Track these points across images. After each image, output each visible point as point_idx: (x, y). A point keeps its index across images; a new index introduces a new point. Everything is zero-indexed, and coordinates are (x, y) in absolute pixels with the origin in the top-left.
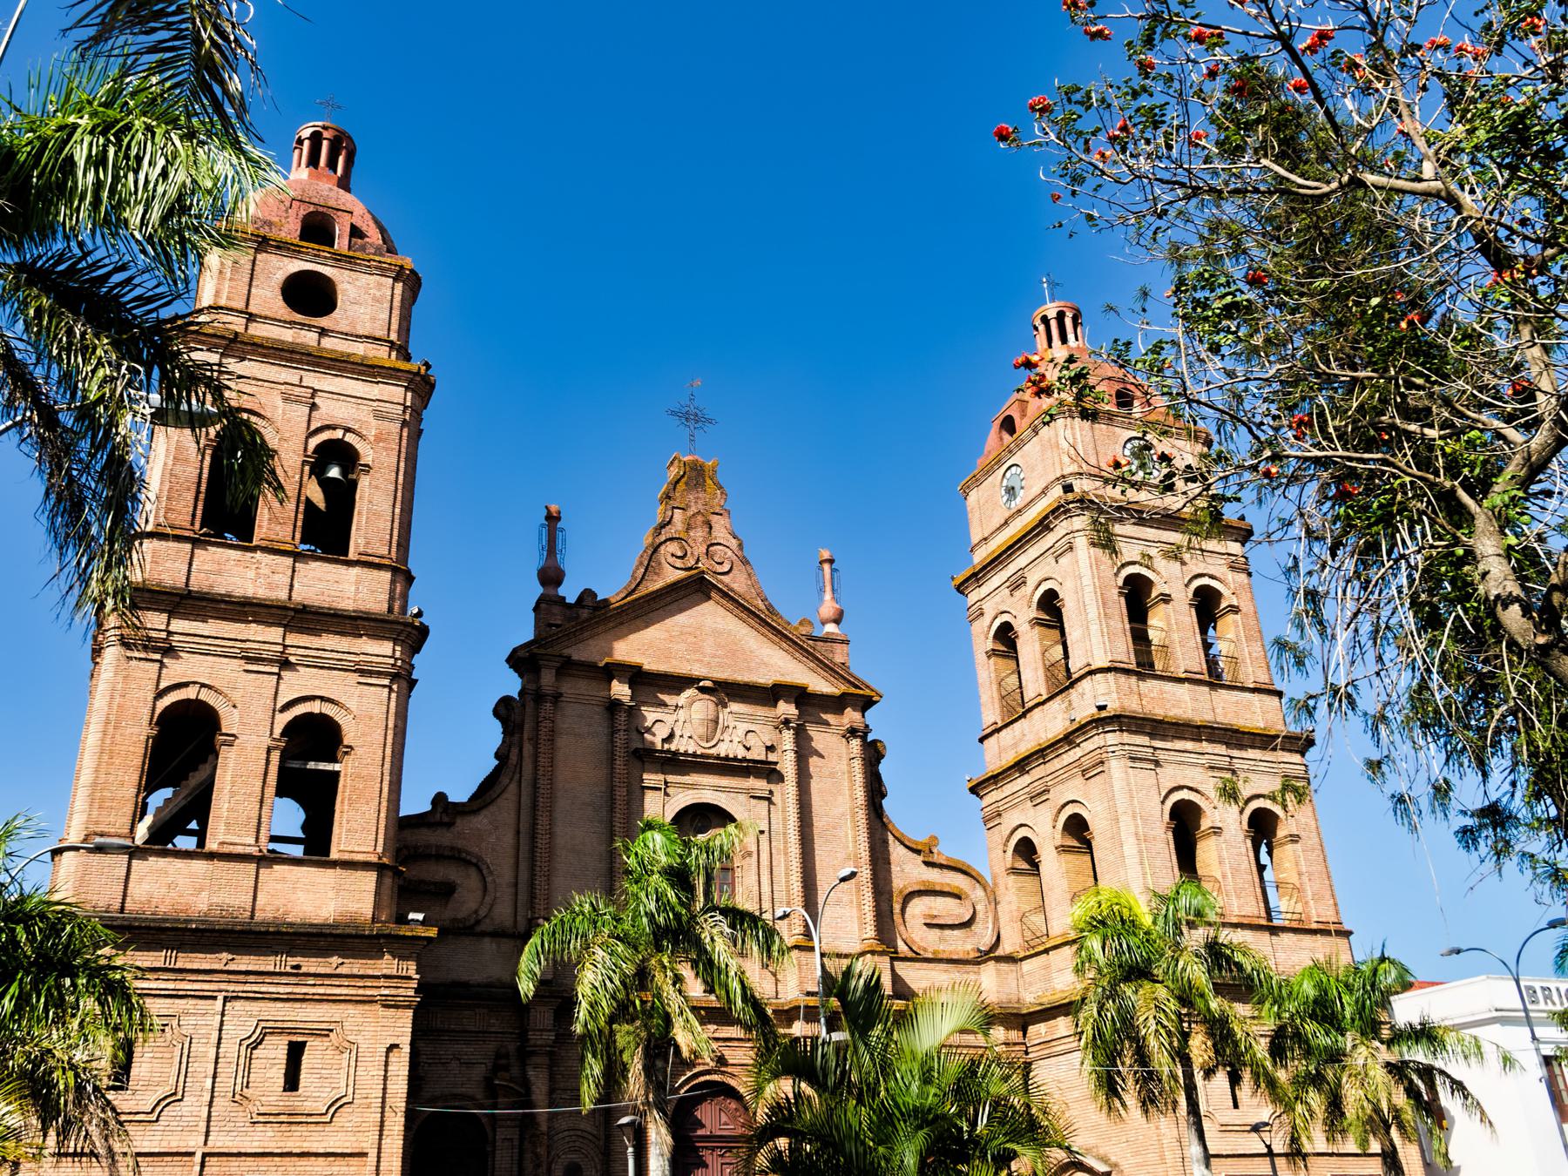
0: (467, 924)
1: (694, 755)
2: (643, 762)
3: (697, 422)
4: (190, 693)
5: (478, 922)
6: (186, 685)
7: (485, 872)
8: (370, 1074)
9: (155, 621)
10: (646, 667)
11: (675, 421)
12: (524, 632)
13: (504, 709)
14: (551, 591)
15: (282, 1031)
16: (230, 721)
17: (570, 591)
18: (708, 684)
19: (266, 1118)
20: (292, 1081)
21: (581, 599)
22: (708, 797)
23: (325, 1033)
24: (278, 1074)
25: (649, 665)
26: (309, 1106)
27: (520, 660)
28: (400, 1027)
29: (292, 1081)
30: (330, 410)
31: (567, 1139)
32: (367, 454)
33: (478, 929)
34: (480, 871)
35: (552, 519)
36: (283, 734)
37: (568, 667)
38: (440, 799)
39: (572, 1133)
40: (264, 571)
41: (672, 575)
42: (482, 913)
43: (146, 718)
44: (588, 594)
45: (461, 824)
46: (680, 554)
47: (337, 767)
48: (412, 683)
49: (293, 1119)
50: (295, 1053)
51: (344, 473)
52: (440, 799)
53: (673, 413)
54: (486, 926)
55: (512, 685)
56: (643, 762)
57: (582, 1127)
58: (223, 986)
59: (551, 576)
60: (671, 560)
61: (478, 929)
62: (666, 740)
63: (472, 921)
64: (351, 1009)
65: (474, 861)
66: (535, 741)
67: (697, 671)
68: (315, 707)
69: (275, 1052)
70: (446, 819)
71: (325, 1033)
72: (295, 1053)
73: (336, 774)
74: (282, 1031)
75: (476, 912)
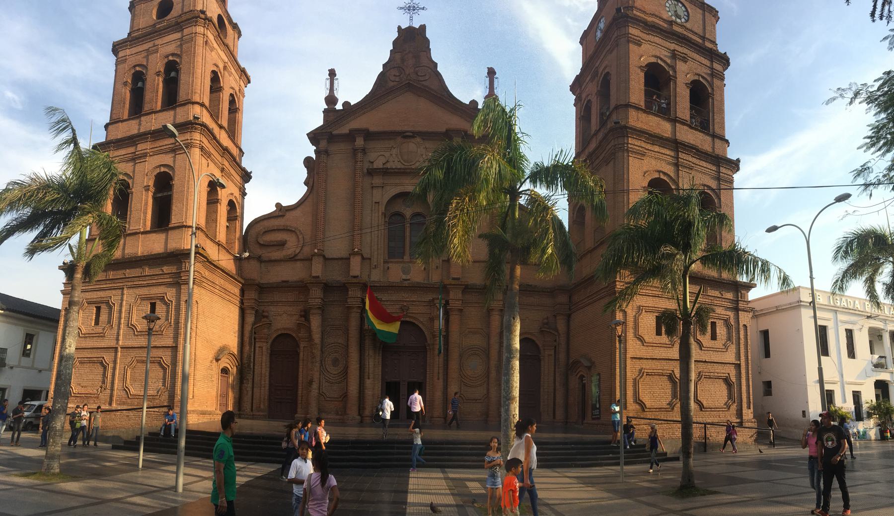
0: (291, 256)
1: (400, 169)
2: (372, 176)
3: (414, 10)
5: (296, 255)
7: (298, 233)
11: (402, 11)
18: (407, 134)
25: (373, 129)
27: (314, 137)
31: (334, 347)
33: (296, 258)
34: (296, 233)
39: (336, 344)
42: (297, 251)
45: (289, 215)
46: (398, 74)
52: (278, 205)
53: (401, 8)
54: (299, 257)
56: (372, 176)
57: (339, 341)
61: (296, 258)
63: (293, 255)
65: (293, 230)
66: (318, 173)
67: (406, 128)
70: (280, 214)
75: (295, 252)
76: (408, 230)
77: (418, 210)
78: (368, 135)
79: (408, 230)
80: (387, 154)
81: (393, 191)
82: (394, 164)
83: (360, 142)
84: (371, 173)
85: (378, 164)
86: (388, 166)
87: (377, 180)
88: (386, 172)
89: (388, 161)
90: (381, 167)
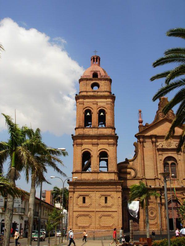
4: (86, 150)
6: (85, 149)
8: (116, 201)
9: (79, 141)
10: (157, 135)
12: (137, 131)
13: (135, 145)
14: (141, 124)
15: (104, 196)
16: (92, 153)
17: (144, 124)
19: (103, 207)
20: (106, 202)
21: (146, 125)
22: (170, 155)
23: (109, 196)
24: (104, 201)
26: (108, 205)
28: (120, 195)
29: (106, 202)
30: (99, 104)
32: (106, 110)
35: (140, 112)
36: (99, 155)
37: (144, 137)
38: (126, 159)
40: (94, 131)
41: (161, 119)
43: (80, 154)
44: (147, 124)
47: (107, 158)
48: (117, 145)
49: (107, 207)
50: (106, 198)
51: (103, 114)
52: (126, 159)
55: (136, 140)
58: (95, 190)
59: (141, 122)
60: (161, 116)
62: (162, 147)
64: (113, 192)
68: (103, 150)
69: (103, 198)
71: (109, 196)
72: (106, 198)
73: (108, 159)
74: (104, 196)
76: (170, 169)
77: (173, 162)
78: (156, 137)
79: (170, 169)
80: (162, 143)
81: (165, 156)
82: (165, 147)
83: (154, 140)
84: (159, 150)
85: (160, 147)
86: (163, 147)
87: (160, 153)
88: (163, 150)
89: (163, 146)
90: (161, 148)
